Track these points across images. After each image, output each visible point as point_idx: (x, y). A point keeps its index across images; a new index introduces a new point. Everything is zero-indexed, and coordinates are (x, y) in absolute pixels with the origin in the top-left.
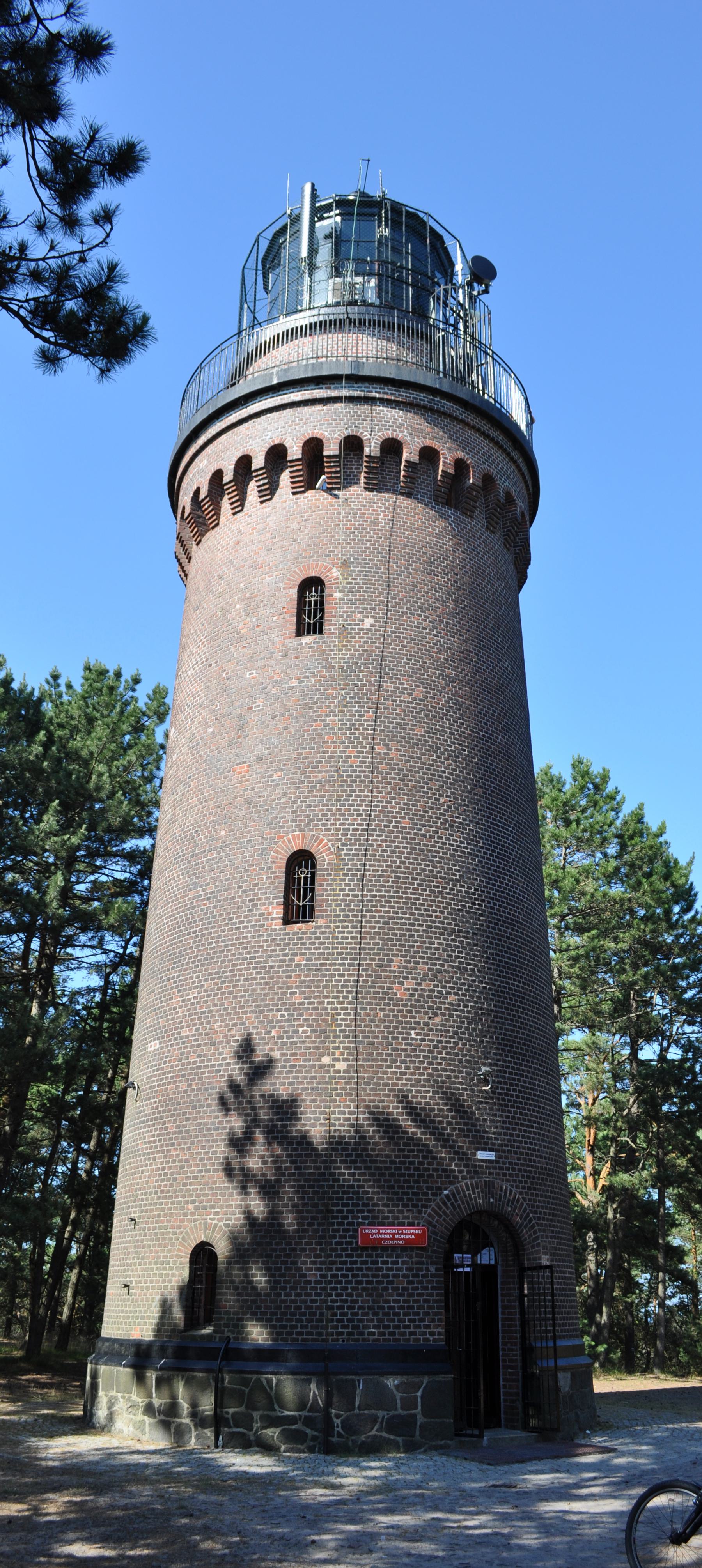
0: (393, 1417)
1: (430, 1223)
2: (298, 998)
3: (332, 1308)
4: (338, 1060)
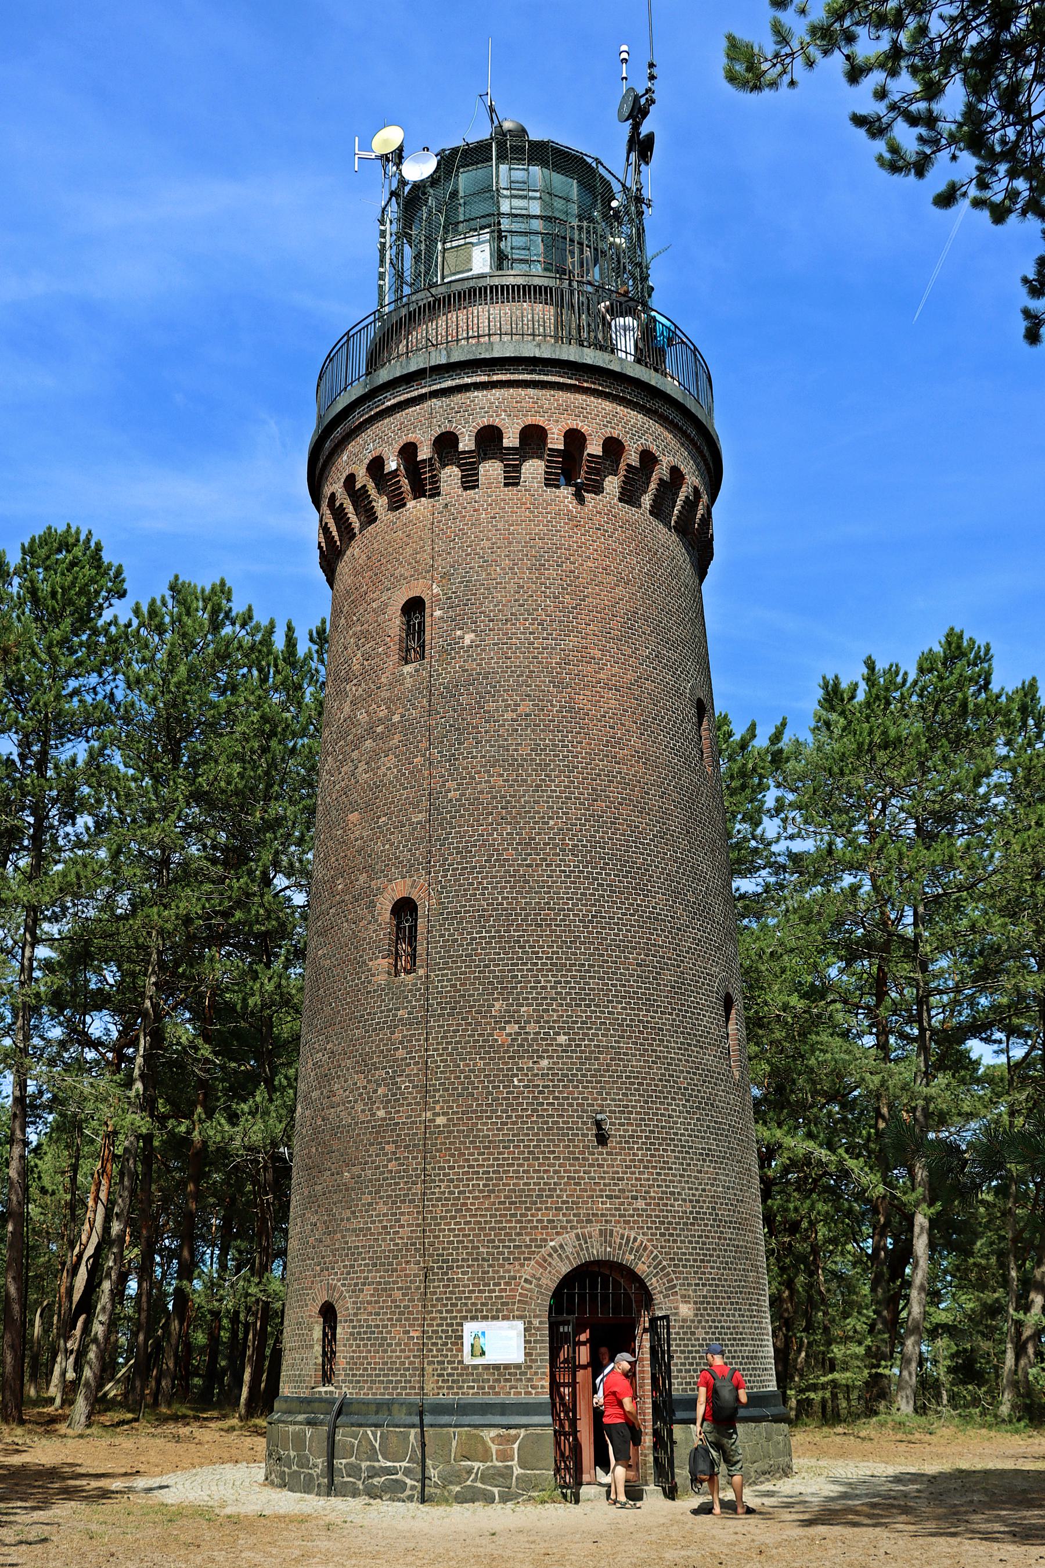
0: (488, 1468)
2: (401, 1053)
4: (438, 1115)
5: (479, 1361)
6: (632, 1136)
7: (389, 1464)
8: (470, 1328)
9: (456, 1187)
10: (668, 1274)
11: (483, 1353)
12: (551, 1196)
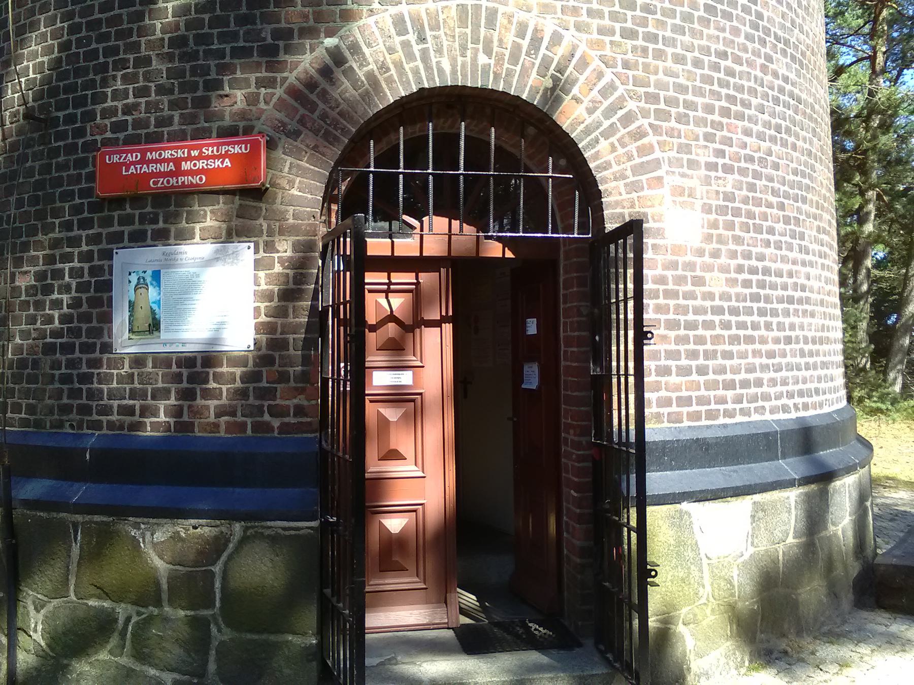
11: (155, 326)
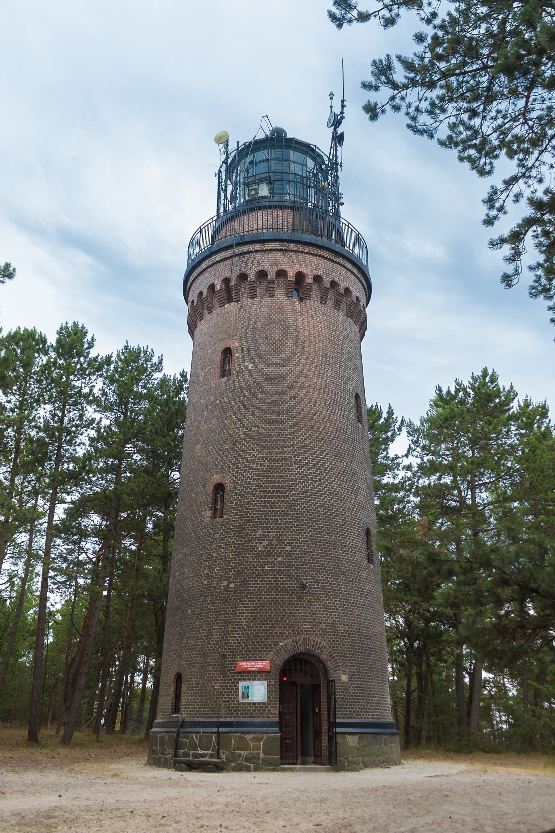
0: (249, 754)
1: (272, 660)
2: (215, 554)
3: (225, 701)
5: (246, 701)
6: (319, 594)
7: (202, 752)
8: (242, 684)
9: (238, 616)
10: (336, 660)
11: (248, 697)
12: (281, 621)
